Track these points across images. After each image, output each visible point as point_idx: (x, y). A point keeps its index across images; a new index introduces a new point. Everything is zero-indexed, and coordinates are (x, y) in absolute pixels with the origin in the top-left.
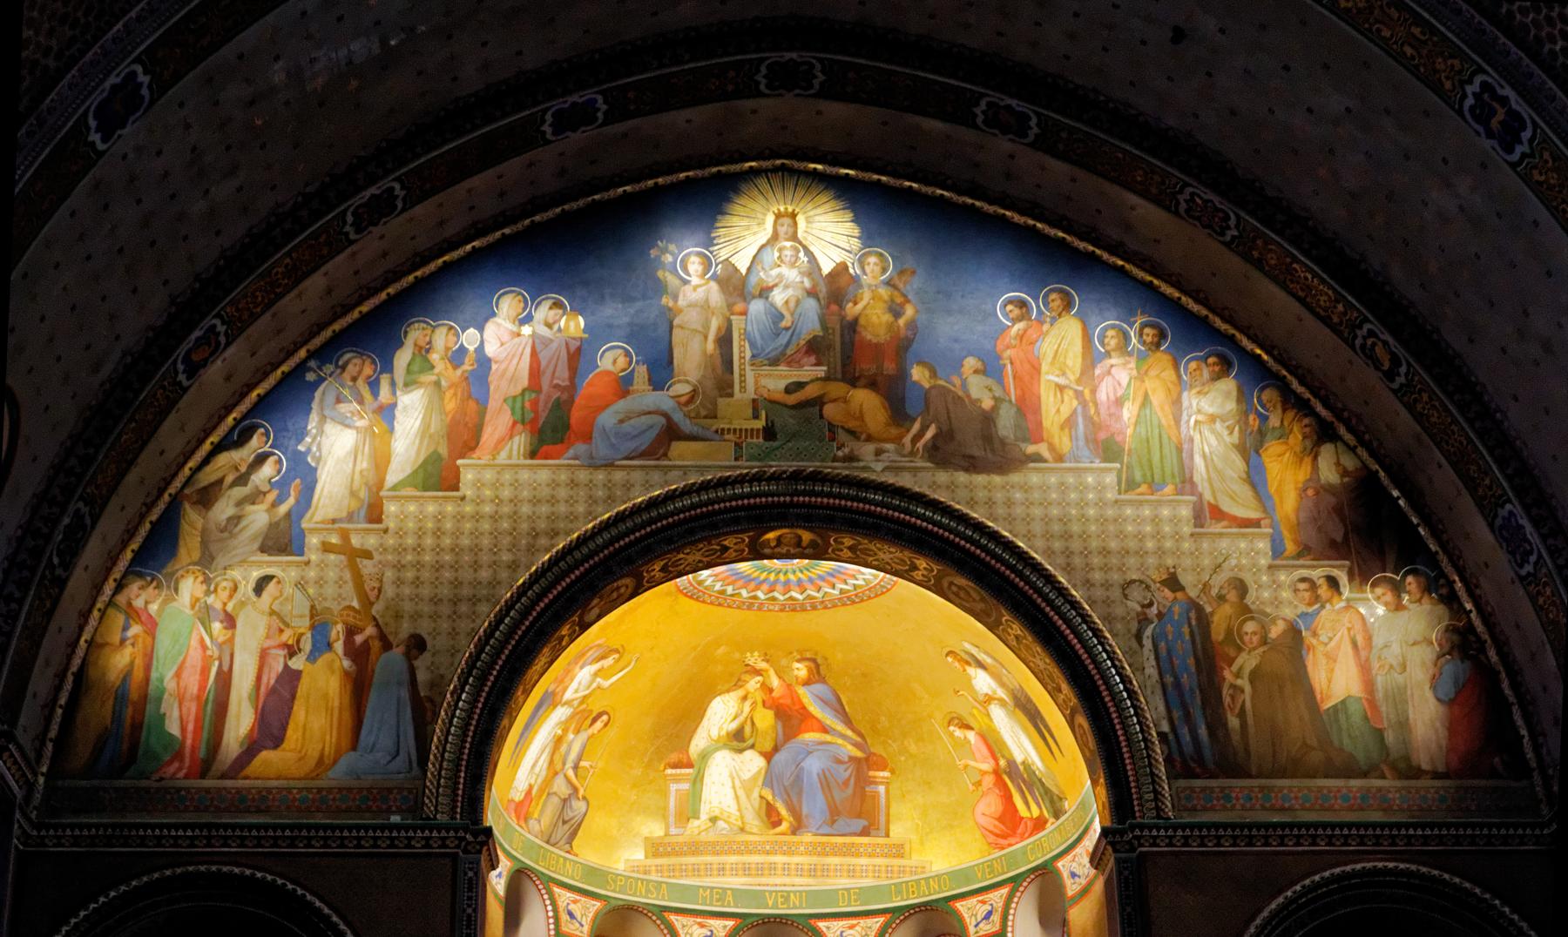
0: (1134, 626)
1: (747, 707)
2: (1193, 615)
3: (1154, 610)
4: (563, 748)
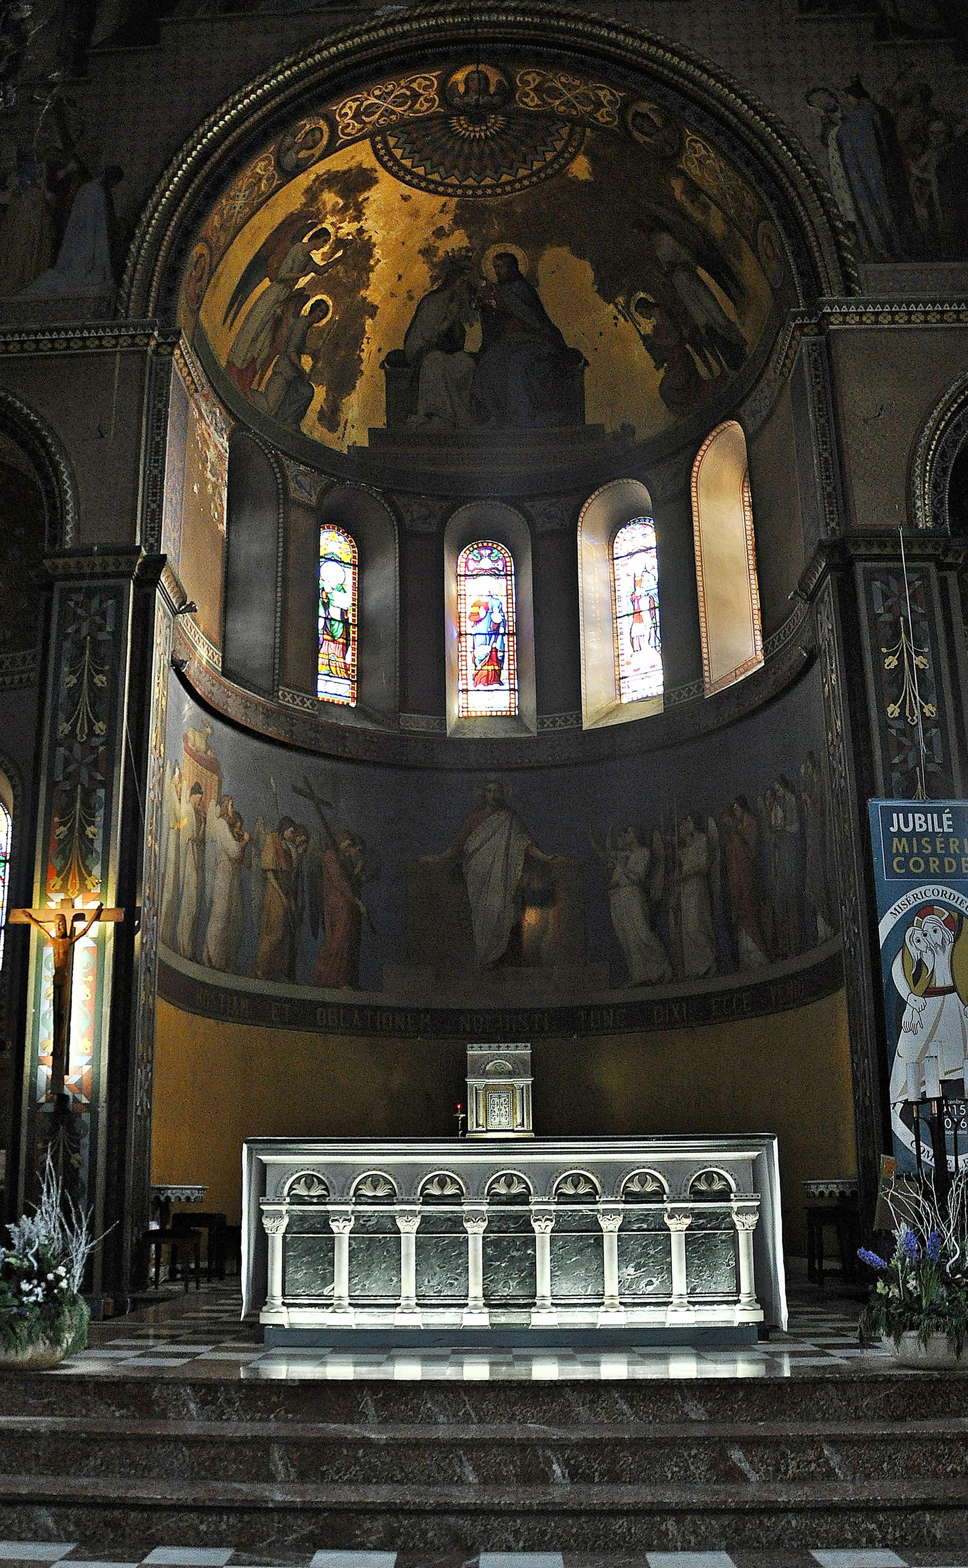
0: (818, 131)
1: (454, 306)
2: (877, 118)
3: (838, 114)
4: (284, 331)
